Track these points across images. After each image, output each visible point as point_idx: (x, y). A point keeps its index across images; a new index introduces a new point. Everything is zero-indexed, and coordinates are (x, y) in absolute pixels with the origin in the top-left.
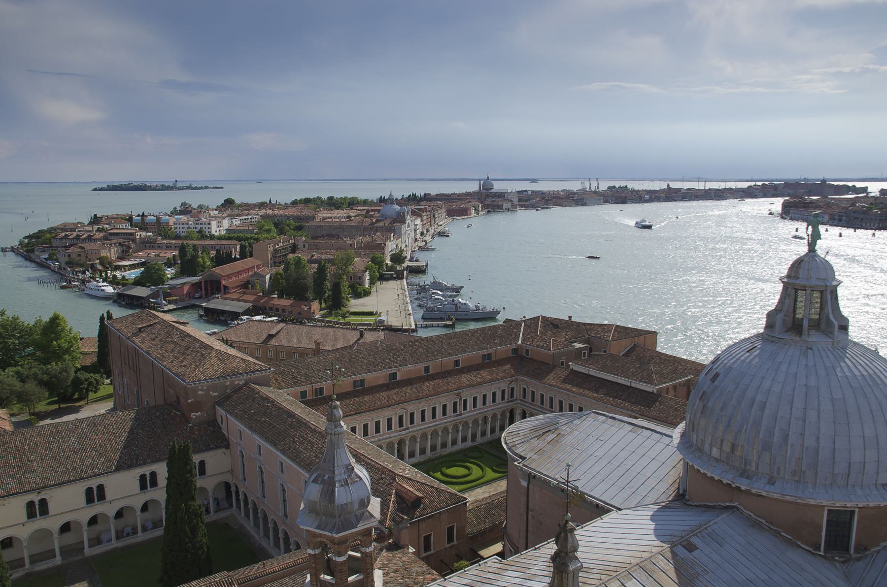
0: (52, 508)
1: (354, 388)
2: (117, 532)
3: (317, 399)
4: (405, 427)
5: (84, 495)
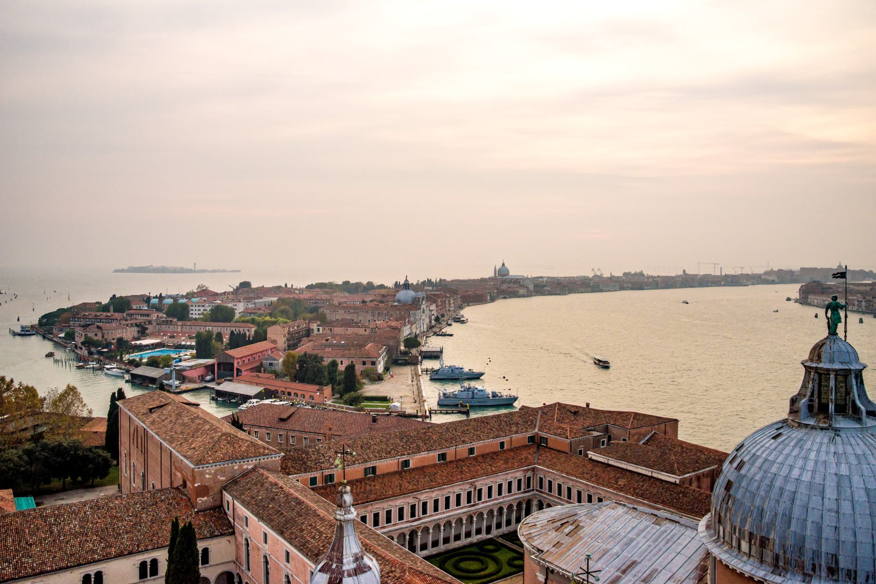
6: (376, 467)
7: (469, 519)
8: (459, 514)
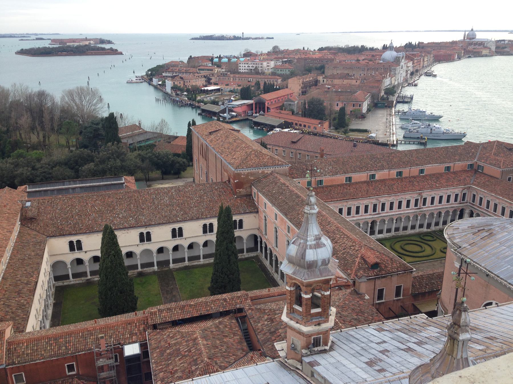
0: (185, 234)
1: (419, 174)
2: (395, 228)
3: (398, 179)
4: (418, 207)
5: (202, 229)
6: (402, 172)
7: (438, 214)
8: (432, 210)
